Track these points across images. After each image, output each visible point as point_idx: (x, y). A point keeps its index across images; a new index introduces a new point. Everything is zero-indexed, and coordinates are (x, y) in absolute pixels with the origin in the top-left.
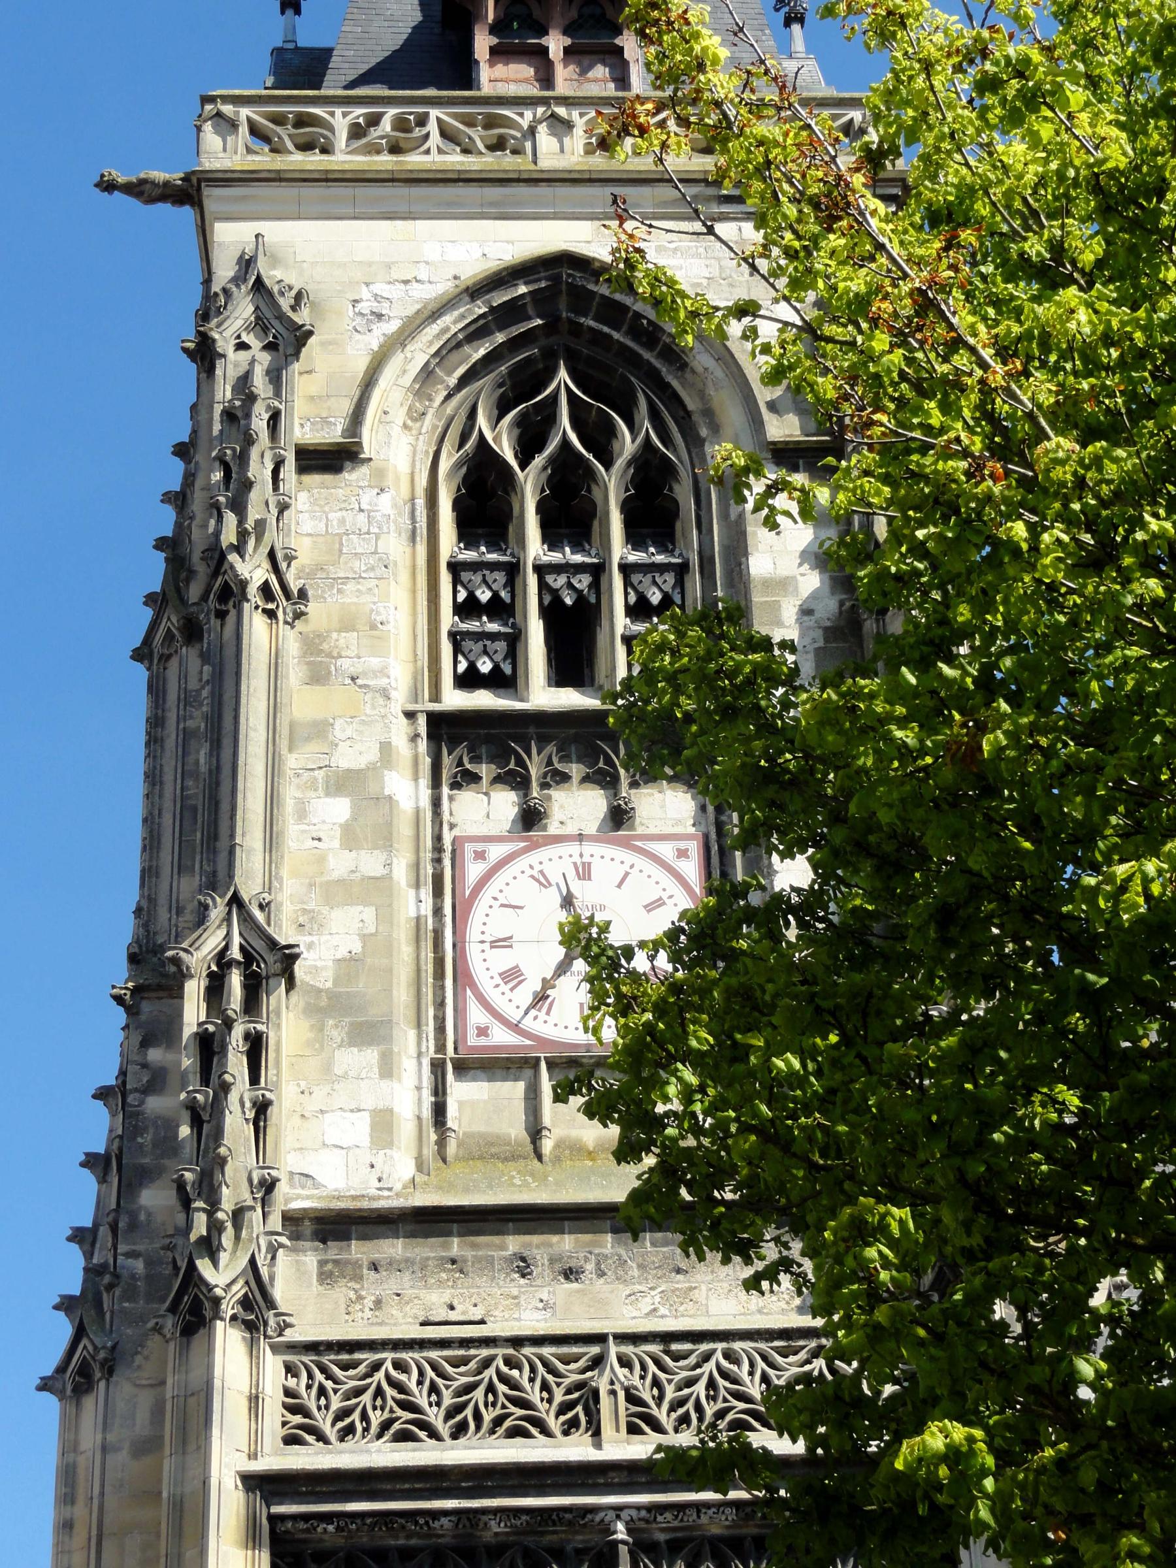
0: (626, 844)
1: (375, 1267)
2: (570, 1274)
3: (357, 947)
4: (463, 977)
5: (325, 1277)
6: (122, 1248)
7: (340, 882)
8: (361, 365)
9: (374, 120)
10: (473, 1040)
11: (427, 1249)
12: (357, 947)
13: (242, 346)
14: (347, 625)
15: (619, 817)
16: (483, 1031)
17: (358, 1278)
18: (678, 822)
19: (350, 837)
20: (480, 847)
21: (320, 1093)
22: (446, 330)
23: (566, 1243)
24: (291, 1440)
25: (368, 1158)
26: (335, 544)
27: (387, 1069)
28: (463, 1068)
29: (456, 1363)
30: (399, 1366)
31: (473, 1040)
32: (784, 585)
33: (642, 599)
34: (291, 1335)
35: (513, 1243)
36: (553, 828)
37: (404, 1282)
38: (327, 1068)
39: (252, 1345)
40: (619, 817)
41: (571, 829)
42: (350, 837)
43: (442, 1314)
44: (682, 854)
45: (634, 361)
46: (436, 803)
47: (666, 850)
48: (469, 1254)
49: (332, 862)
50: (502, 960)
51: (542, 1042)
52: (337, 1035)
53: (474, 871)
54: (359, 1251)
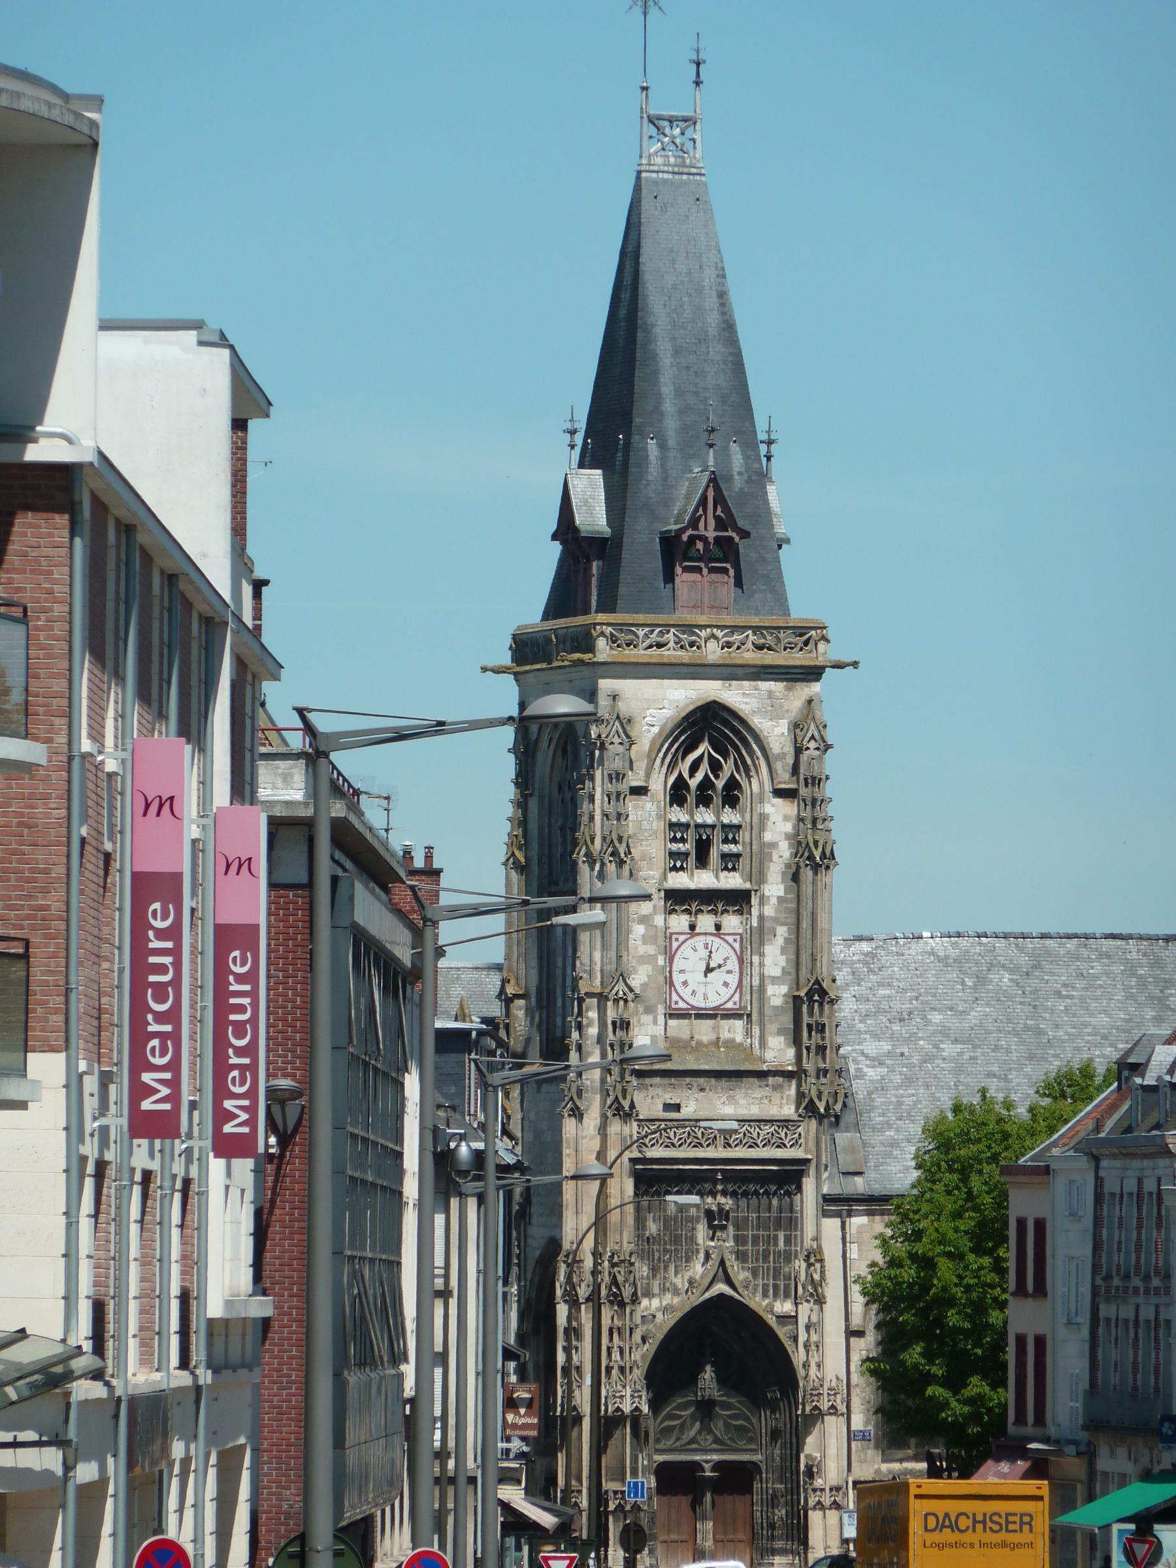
0: (718, 935)
2: (702, 1090)
3: (646, 980)
4: (672, 984)
9: (652, 632)
11: (666, 1081)
12: (646, 980)
14: (643, 859)
15: (718, 927)
17: (647, 1089)
18: (734, 928)
20: (676, 936)
23: (702, 1080)
26: (639, 823)
27: (655, 1022)
28: (671, 1016)
31: (673, 1006)
32: (774, 845)
33: (727, 837)
34: (641, 1117)
35: (688, 1080)
37: (659, 1091)
40: (718, 927)
41: (702, 931)
42: (645, 941)
44: (735, 940)
47: (730, 939)
48: (676, 1082)
50: (682, 977)
51: (693, 1008)
52: (641, 1010)
53: (675, 945)
54: (648, 1081)
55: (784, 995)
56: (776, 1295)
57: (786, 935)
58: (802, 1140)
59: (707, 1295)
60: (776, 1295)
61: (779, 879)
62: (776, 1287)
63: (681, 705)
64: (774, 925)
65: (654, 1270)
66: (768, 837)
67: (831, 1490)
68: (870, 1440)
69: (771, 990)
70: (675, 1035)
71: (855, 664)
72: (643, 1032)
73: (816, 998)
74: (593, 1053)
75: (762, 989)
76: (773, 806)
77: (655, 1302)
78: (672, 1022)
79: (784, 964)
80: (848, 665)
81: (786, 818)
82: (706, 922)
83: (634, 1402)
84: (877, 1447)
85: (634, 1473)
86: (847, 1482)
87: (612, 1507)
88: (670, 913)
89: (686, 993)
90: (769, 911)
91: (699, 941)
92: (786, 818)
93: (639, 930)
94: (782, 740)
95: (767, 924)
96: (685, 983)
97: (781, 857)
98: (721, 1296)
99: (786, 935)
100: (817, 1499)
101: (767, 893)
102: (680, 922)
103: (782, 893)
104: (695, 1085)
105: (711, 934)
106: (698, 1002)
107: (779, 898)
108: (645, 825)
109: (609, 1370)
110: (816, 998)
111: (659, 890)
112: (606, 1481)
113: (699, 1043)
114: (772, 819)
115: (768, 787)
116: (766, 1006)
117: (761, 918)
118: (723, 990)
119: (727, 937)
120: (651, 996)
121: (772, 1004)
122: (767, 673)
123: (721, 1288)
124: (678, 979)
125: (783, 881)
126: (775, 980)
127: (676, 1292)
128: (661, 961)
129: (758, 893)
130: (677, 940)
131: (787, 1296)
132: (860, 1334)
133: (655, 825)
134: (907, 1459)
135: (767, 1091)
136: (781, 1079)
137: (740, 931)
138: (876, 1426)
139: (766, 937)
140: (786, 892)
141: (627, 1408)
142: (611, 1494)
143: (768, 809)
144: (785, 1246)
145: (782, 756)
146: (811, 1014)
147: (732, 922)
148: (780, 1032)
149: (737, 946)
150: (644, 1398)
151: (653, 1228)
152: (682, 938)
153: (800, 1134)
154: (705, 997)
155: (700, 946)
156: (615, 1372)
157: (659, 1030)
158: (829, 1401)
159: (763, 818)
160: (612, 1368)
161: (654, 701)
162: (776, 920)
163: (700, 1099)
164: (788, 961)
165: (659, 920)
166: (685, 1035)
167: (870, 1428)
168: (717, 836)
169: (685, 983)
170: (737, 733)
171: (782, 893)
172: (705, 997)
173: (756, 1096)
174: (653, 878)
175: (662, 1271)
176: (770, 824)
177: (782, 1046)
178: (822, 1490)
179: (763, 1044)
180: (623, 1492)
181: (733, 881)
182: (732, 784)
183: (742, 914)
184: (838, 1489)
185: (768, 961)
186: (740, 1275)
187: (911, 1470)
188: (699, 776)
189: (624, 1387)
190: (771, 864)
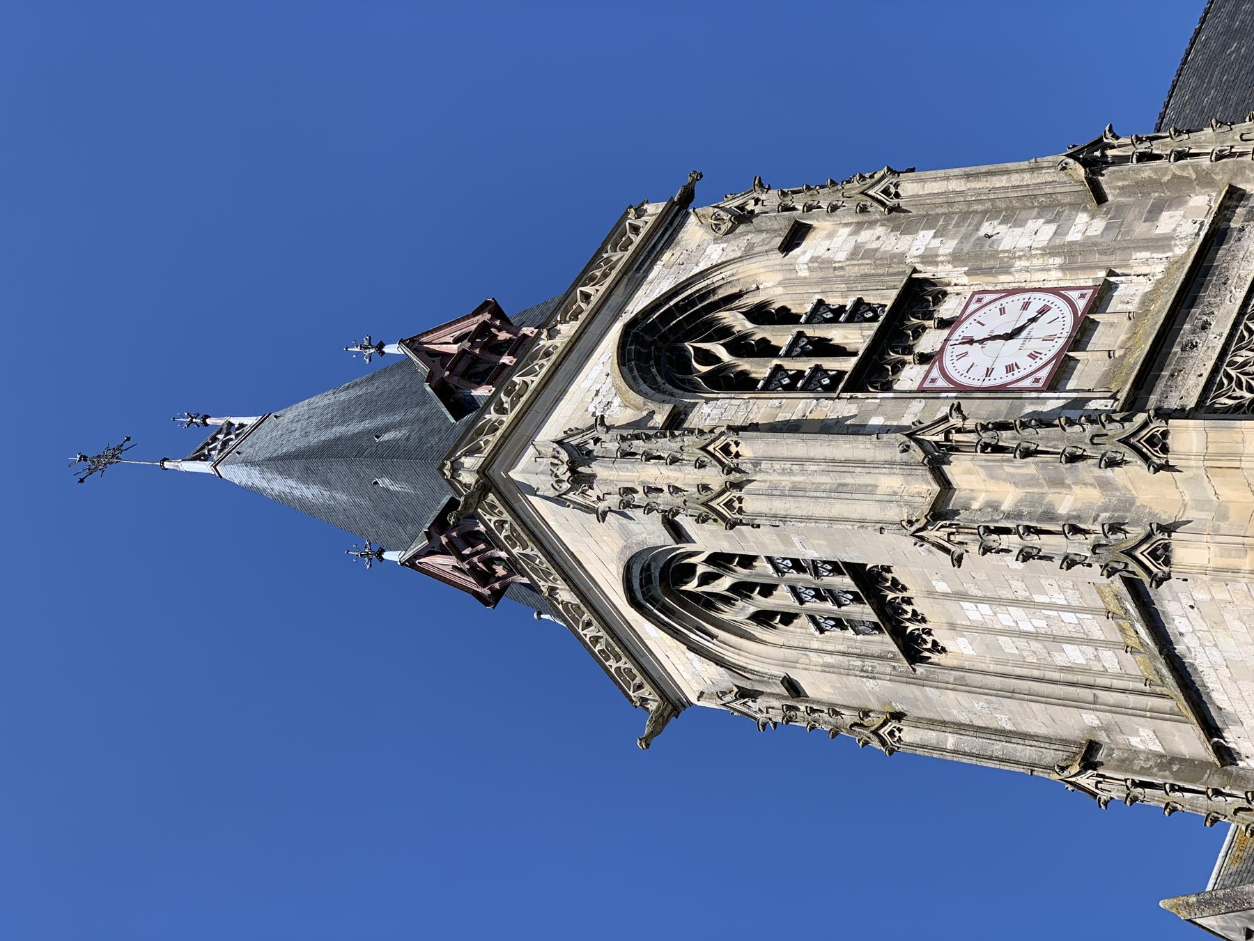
18: (960, 304)
20: (928, 380)
44: (979, 300)
45: (698, 314)
47: (973, 307)
55: (1093, 218)
57: (996, 222)
61: (908, 237)
69: (1074, 235)
73: (1098, 154)
74: (1051, 504)
79: (1042, 221)
81: (831, 236)
82: (930, 341)
89: (1027, 365)
90: (948, 246)
96: (1009, 369)
102: (910, 376)
103: (932, 232)
105: (951, 334)
110: (1098, 154)
114: (821, 251)
115: (777, 257)
117: (956, 258)
122: (639, 269)
129: (919, 267)
130: (933, 380)
136: (1239, 210)
164: (1039, 216)
170: (690, 301)
171: (932, 232)
172: (1050, 338)
176: (827, 255)
183: (945, 294)
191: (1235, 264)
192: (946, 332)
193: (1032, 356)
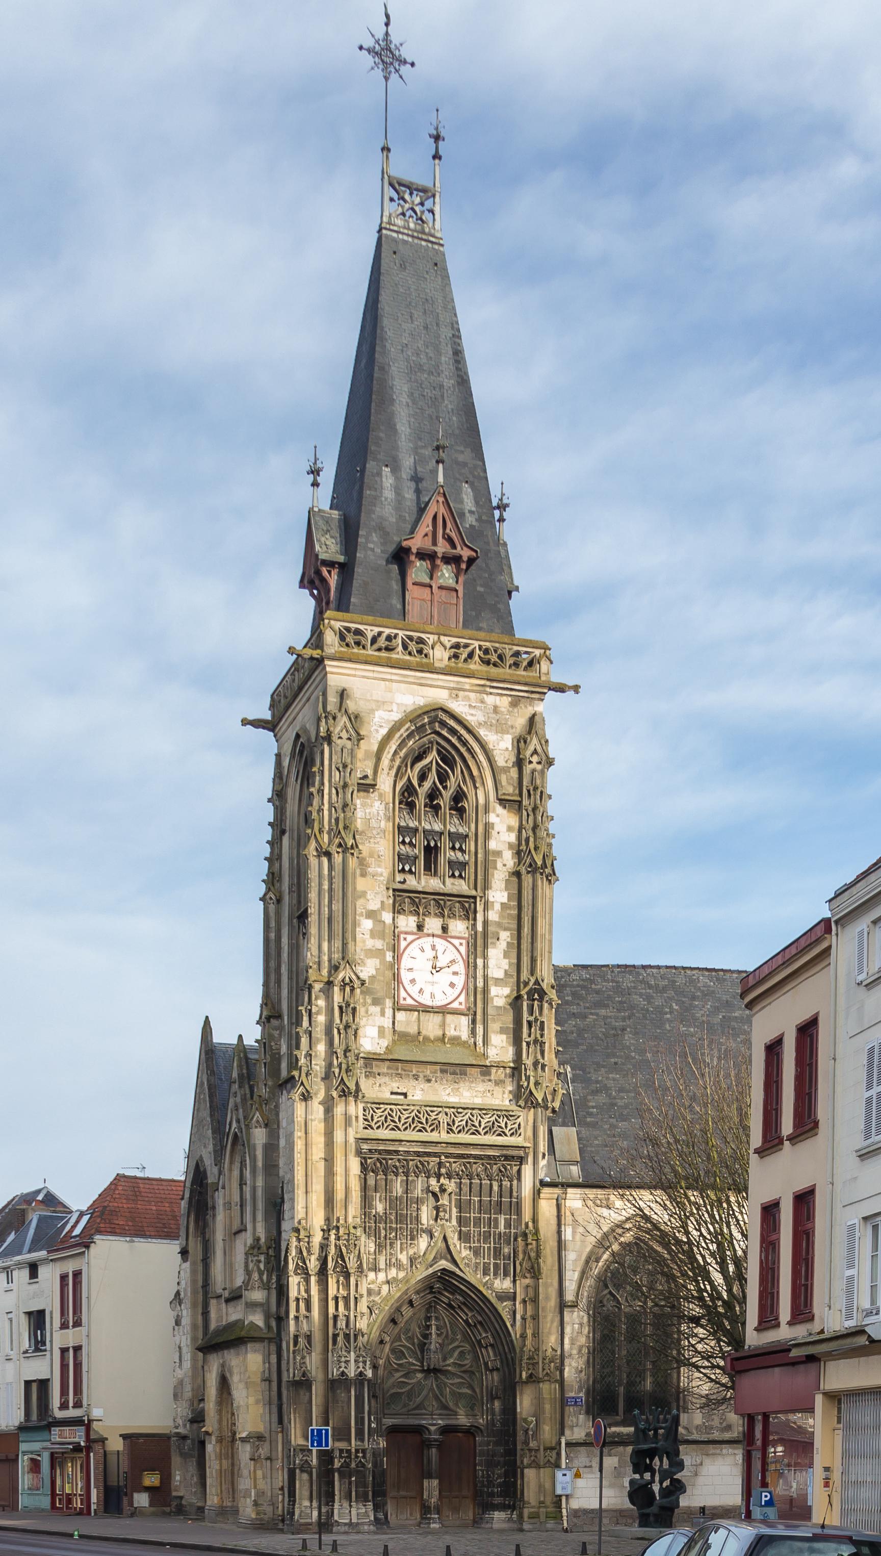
1: (379, 1074)
2: (429, 1081)
3: (374, 973)
5: (366, 1076)
6: (313, 1062)
7: (370, 950)
8: (375, 747)
10: (402, 1002)
12: (374, 973)
13: (340, 738)
15: (445, 929)
16: (405, 999)
17: (375, 1077)
18: (460, 932)
19: (373, 934)
21: (364, 1019)
22: (402, 735)
23: (428, 1071)
24: (365, 1128)
25: (377, 1041)
27: (383, 1014)
28: (399, 1010)
29: (405, 1110)
30: (391, 1109)
31: (402, 1002)
32: (499, 854)
36: (425, 931)
37: (387, 1079)
38: (367, 1012)
39: (356, 1101)
40: (445, 929)
41: (430, 932)
43: (396, 1090)
46: (394, 919)
47: (456, 942)
49: (367, 943)
52: (369, 1001)
53: (403, 944)
56: (495, 1274)
57: (509, 940)
58: (522, 1130)
59: (431, 1271)
60: (496, 1274)
61: (503, 886)
62: (496, 1266)
63: (409, 709)
64: (497, 930)
65: (380, 1247)
66: (493, 845)
67: (545, 1449)
68: (582, 1406)
69: (494, 991)
70: (403, 1029)
71: (576, 689)
72: (370, 1022)
75: (485, 991)
76: (498, 816)
77: (382, 1276)
78: (401, 1016)
79: (507, 967)
80: (570, 688)
81: (510, 829)
82: (433, 924)
83: (358, 1367)
84: (588, 1413)
85: (360, 1435)
86: (560, 1444)
87: (337, 1464)
88: (399, 912)
89: (413, 990)
91: (426, 942)
92: (510, 829)
93: (367, 924)
94: (507, 754)
95: (491, 929)
96: (413, 981)
97: (505, 865)
98: (444, 1270)
99: (509, 940)
100: (532, 1458)
101: (491, 899)
102: (407, 922)
103: (505, 900)
104: (421, 1075)
105: (438, 936)
106: (426, 1000)
107: (502, 904)
108: (373, 823)
109: (335, 1336)
110: (536, 996)
111: (388, 889)
112: (333, 1441)
113: (426, 1039)
114: (497, 828)
116: (490, 1005)
117: (486, 923)
118: (449, 990)
119: (453, 941)
120: (379, 988)
121: (495, 1004)
123: (444, 1264)
124: (405, 976)
125: (506, 889)
126: (498, 982)
127: (399, 1266)
128: (389, 956)
130: (405, 939)
131: (506, 1274)
132: (574, 1305)
133: (383, 824)
134: (617, 1424)
135: (490, 1086)
137: (467, 935)
138: (587, 1394)
139: (490, 941)
140: (509, 899)
141: (352, 1372)
142: (337, 1454)
143: (492, 818)
144: (505, 1228)
145: (506, 770)
146: (531, 1012)
147: (458, 927)
148: (502, 1031)
149: (463, 949)
150: (368, 1363)
151: (380, 1207)
152: (410, 938)
153: (519, 1125)
154: (432, 996)
155: (428, 948)
156: (340, 1339)
157: (387, 1022)
158: (544, 1369)
159: (488, 827)
160: (338, 1335)
161: (384, 703)
162: (499, 924)
163: (426, 1088)
164: (510, 964)
165: (387, 917)
166: (413, 1030)
167: (581, 1395)
168: (445, 843)
169: (413, 981)
171: (505, 900)
172: (432, 996)
173: (479, 1089)
174: (381, 875)
175: (388, 1247)
176: (494, 833)
177: (504, 1044)
178: (537, 1450)
179: (486, 1041)
180: (349, 1451)
181: (461, 887)
182: (459, 797)
184: (552, 1449)
185: (492, 963)
186: (463, 1252)
187: (619, 1434)
188: (427, 785)
189: (349, 1352)
190: (496, 872)
191: (467, 1084)
192: (440, 932)
193: (421, 991)
